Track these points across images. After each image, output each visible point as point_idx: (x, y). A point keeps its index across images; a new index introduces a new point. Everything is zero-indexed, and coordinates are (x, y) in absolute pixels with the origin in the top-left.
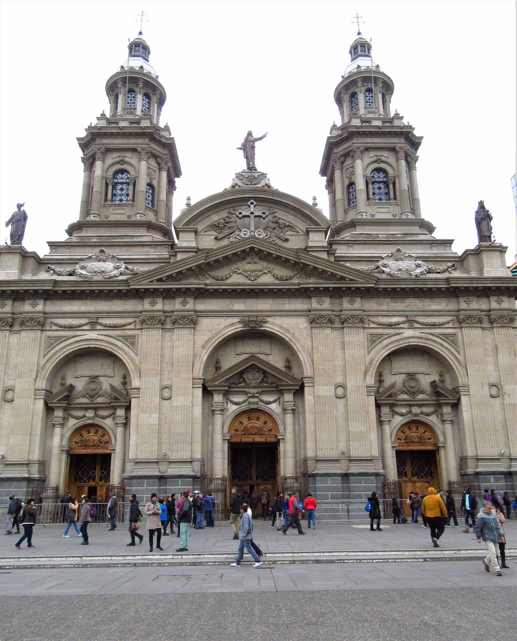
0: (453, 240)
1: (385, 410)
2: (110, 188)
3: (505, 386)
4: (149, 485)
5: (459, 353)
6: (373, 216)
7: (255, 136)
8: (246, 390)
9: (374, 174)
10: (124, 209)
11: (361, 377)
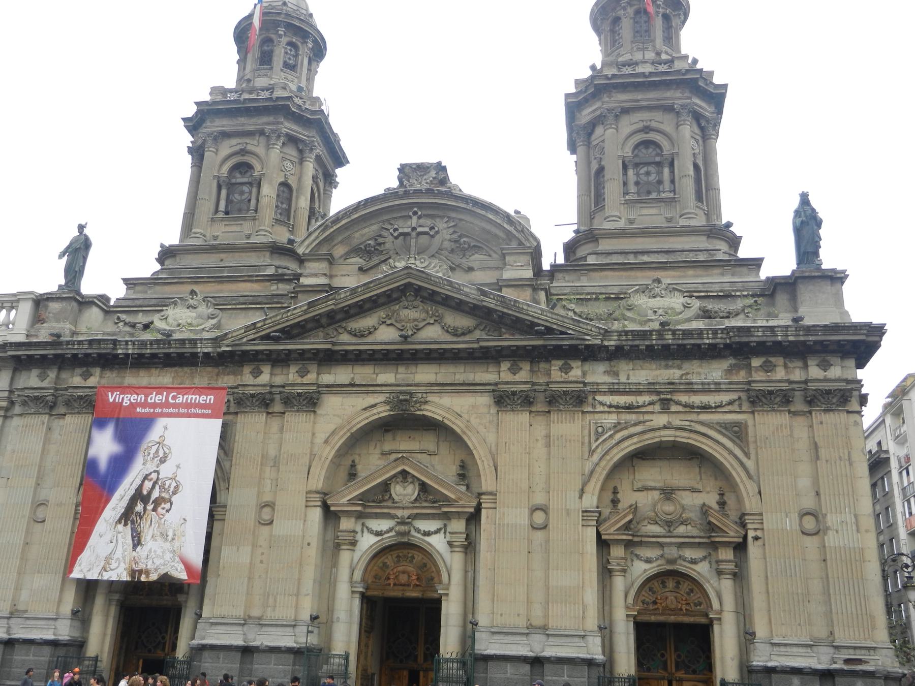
0: (762, 259)
1: (617, 552)
2: (224, 192)
3: (829, 515)
4: (226, 661)
5: (747, 455)
6: (631, 222)
8: (392, 511)
9: (640, 151)
10: (241, 224)
11: (577, 495)
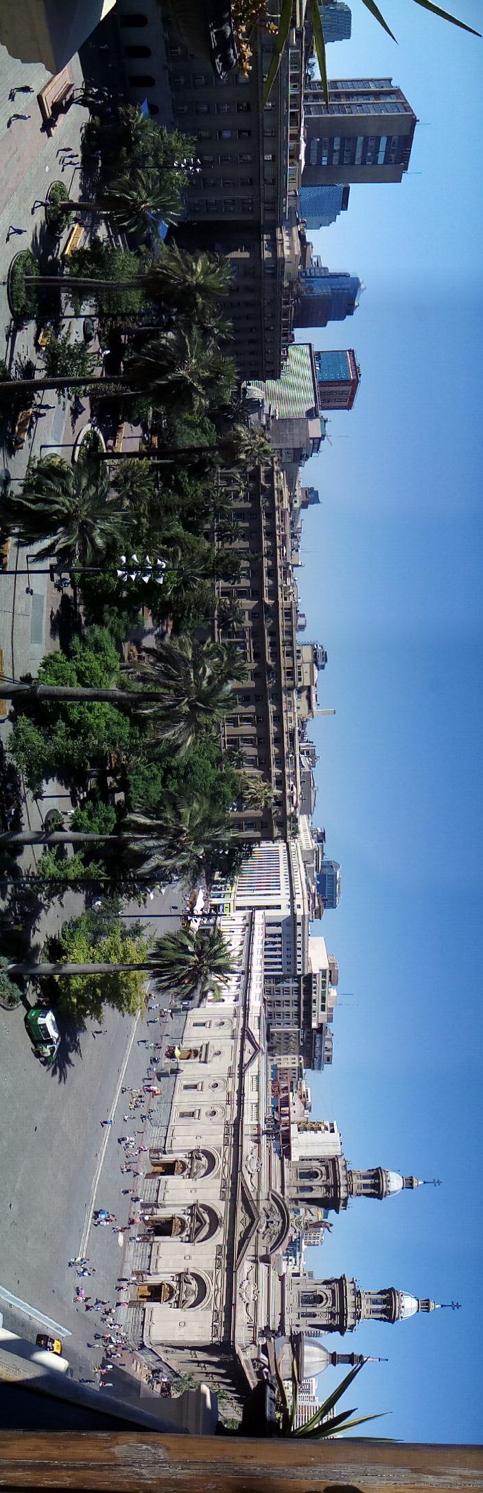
7: (330, 1228)
